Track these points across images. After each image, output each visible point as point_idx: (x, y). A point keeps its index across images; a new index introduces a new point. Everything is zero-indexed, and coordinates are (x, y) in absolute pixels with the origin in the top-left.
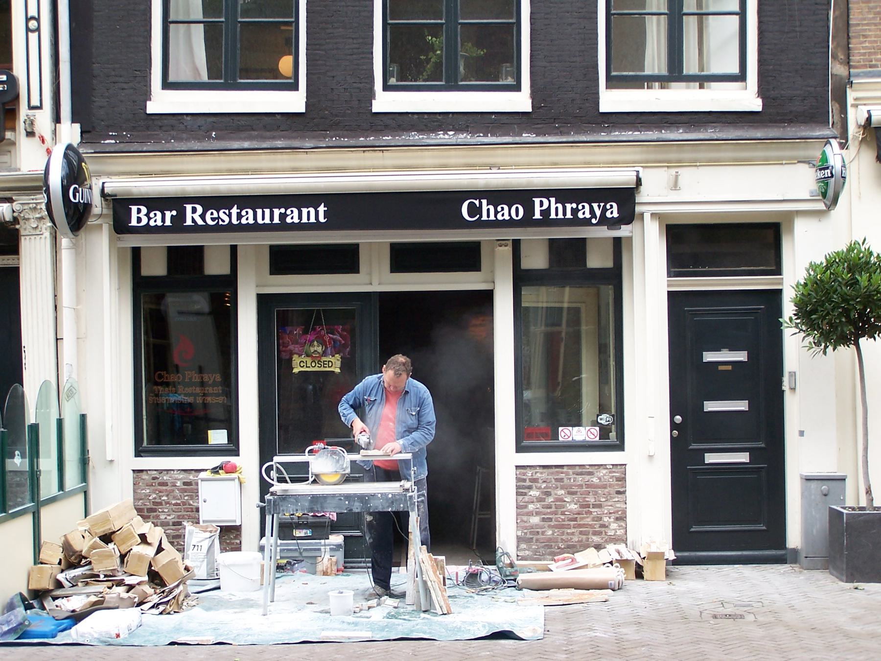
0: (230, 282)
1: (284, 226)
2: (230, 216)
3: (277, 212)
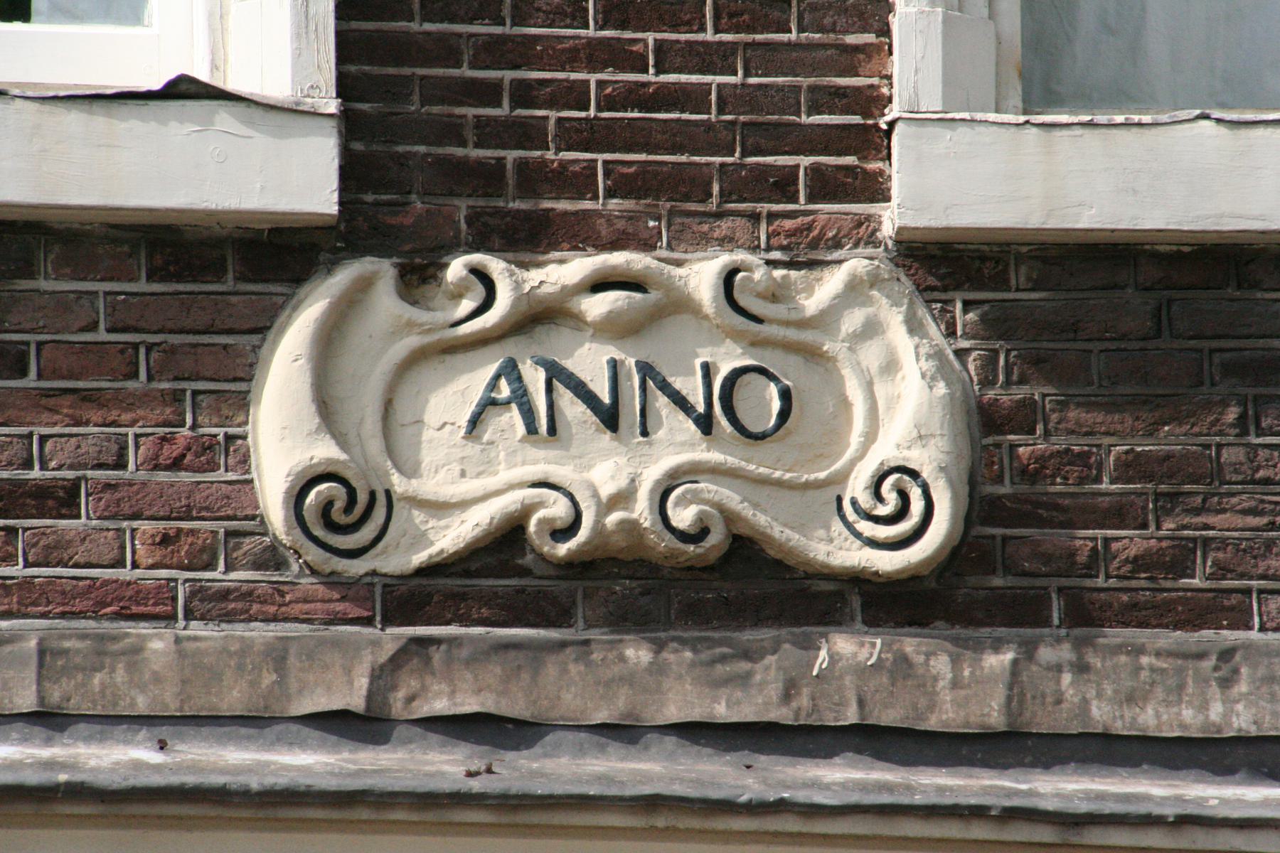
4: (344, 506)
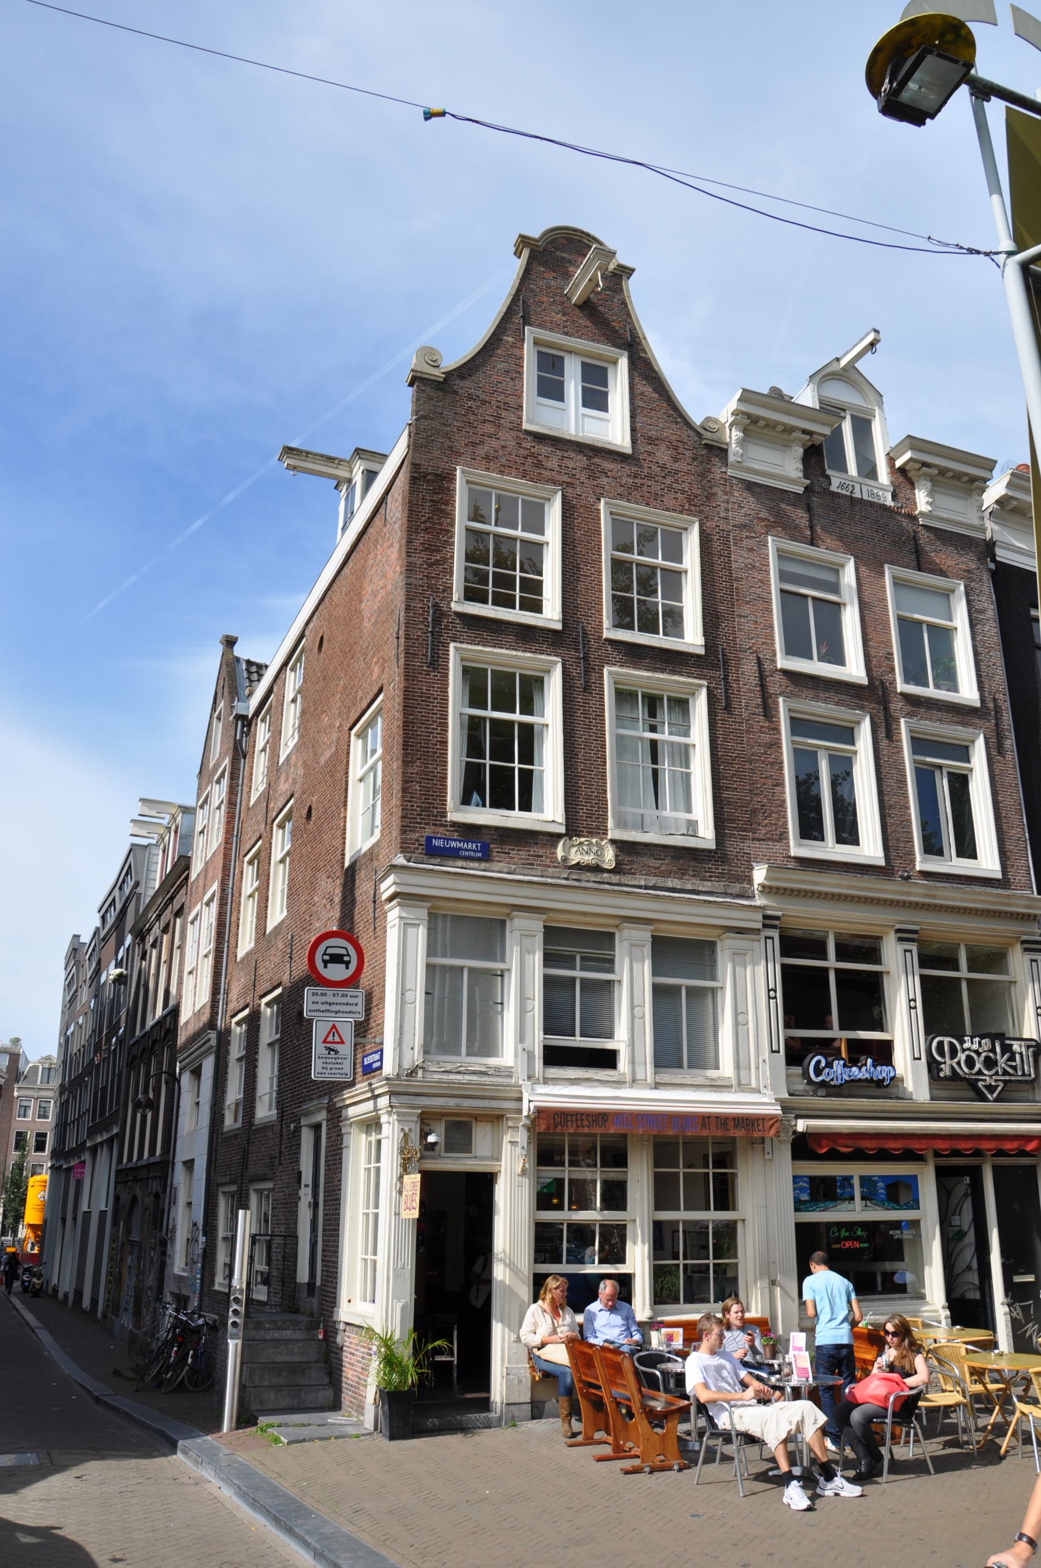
4: (565, 859)
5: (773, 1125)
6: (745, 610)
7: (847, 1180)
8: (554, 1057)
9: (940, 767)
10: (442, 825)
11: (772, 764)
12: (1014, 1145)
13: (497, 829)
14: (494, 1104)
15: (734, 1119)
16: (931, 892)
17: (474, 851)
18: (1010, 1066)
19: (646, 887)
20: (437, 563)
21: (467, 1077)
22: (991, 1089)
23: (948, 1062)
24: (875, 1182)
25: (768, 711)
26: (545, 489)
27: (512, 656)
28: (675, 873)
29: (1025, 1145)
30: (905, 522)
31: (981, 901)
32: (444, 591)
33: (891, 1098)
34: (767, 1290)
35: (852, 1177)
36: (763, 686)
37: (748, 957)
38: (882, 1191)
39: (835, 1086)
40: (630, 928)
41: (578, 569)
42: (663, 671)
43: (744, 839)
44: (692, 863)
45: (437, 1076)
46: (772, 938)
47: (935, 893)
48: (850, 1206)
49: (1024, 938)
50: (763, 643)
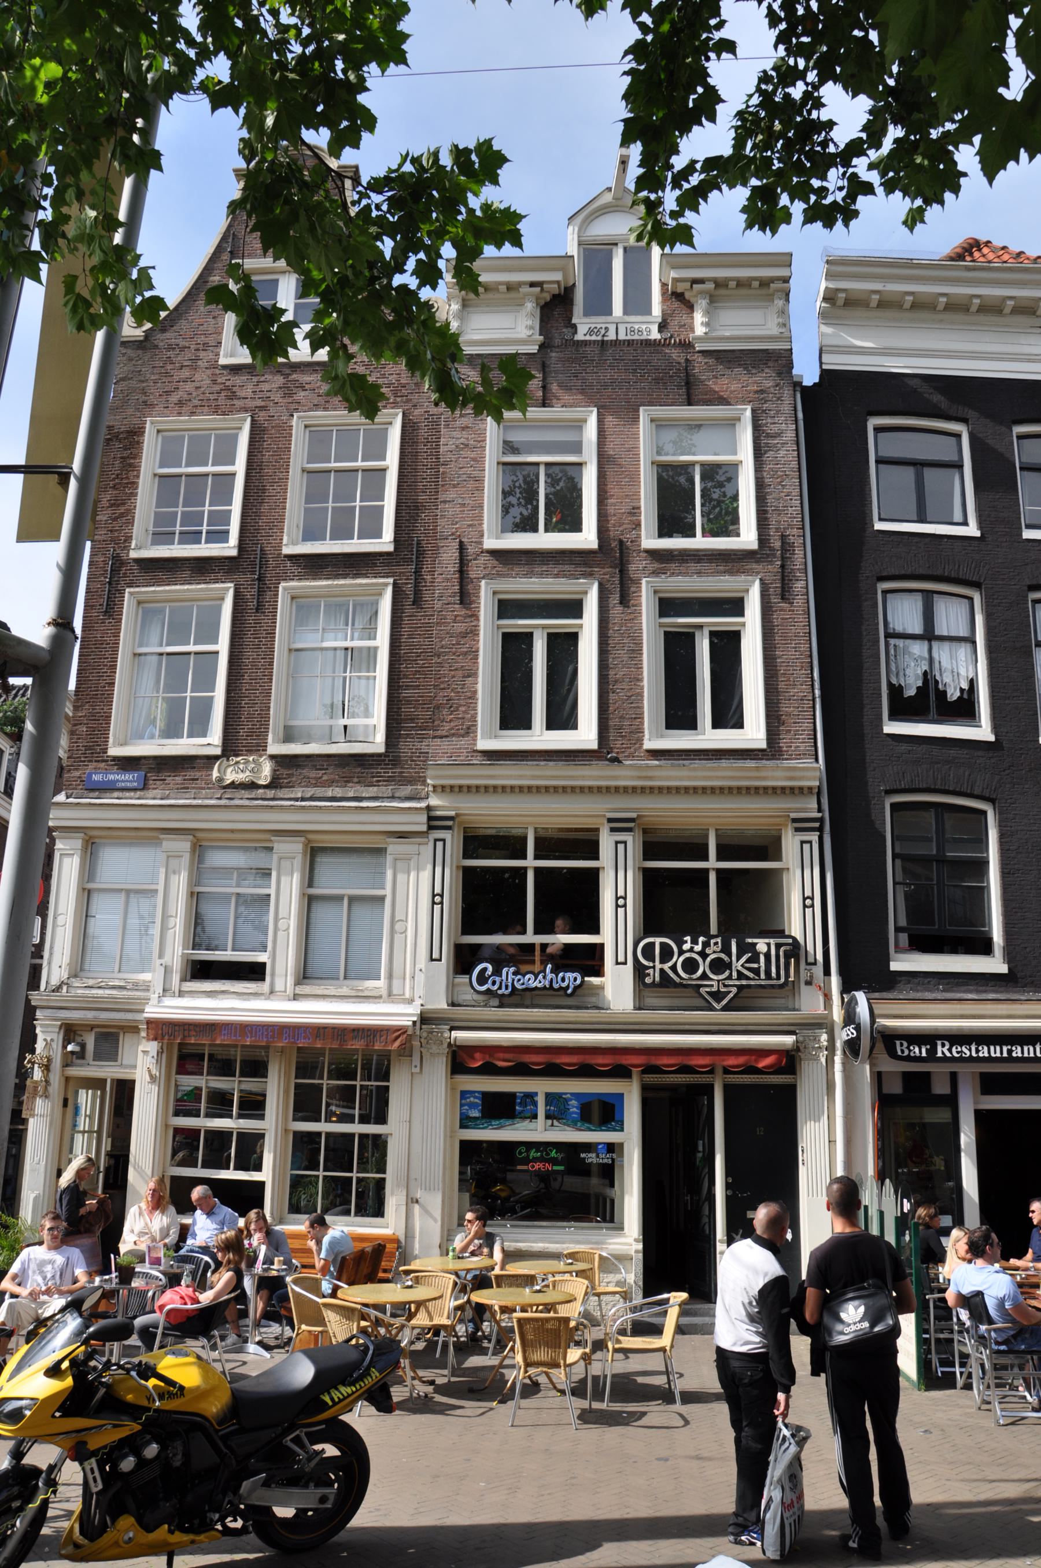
0: (951, 1101)
1: (1010, 1059)
2: (970, 1050)
3: (1005, 1049)
4: (220, 780)
5: (399, 1036)
6: (451, 495)
7: (530, 1097)
8: (201, 970)
9: (700, 627)
10: (103, 761)
11: (466, 653)
12: (741, 1060)
13: (155, 758)
14: (129, 1016)
15: (354, 1030)
16: (644, 774)
17: (131, 781)
18: (749, 969)
19: (303, 799)
20: (122, 515)
21: (108, 992)
22: (718, 996)
23: (658, 966)
24: (566, 1100)
25: (466, 597)
26: (234, 420)
27: (185, 591)
28: (337, 781)
29: (756, 1061)
30: (676, 355)
31: (724, 778)
32: (125, 541)
33: (587, 1008)
34: (404, 1208)
35: (536, 1094)
36: (462, 572)
37: (412, 863)
38: (575, 1109)
39: (503, 995)
40: (279, 842)
41: (264, 490)
42: (345, 576)
43: (423, 738)
44: (358, 770)
45: (80, 991)
46: (444, 840)
47: (650, 773)
48: (532, 1125)
49: (793, 815)
50: (470, 526)
